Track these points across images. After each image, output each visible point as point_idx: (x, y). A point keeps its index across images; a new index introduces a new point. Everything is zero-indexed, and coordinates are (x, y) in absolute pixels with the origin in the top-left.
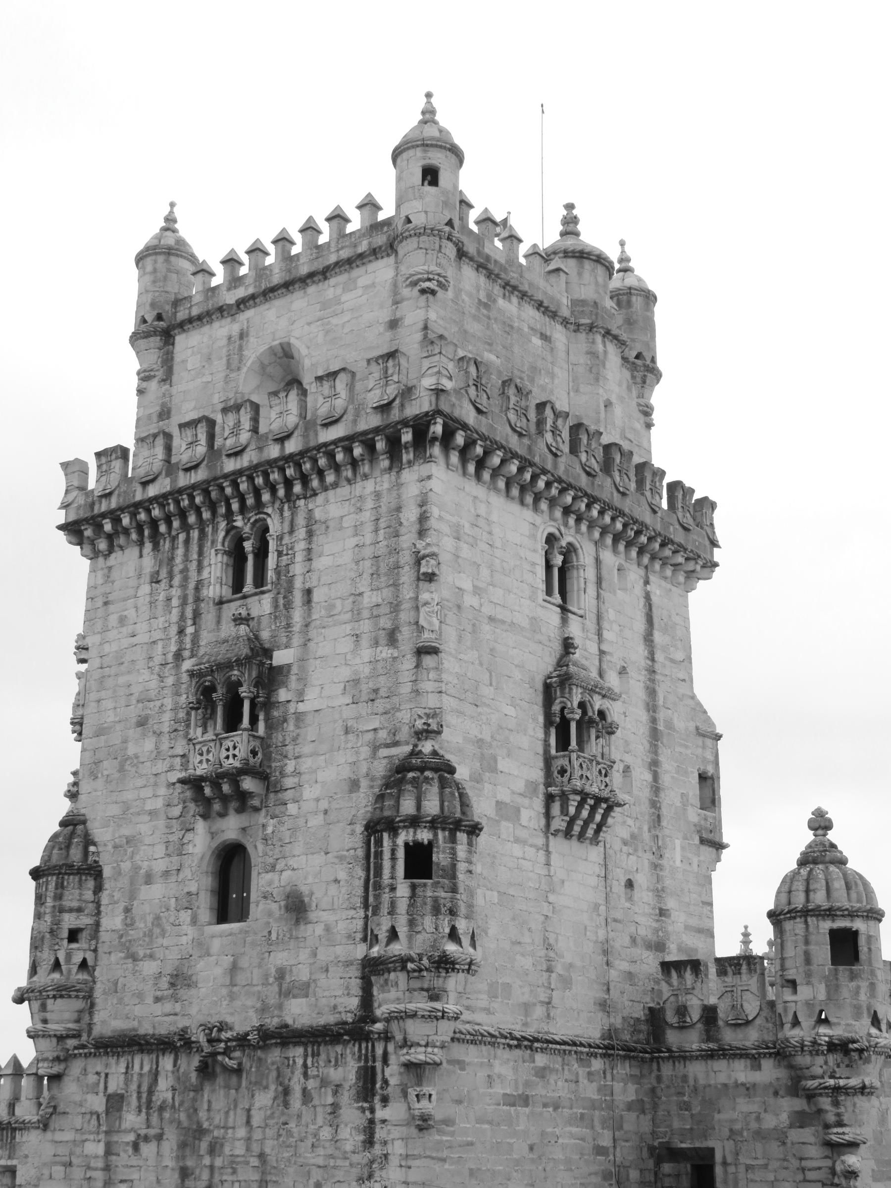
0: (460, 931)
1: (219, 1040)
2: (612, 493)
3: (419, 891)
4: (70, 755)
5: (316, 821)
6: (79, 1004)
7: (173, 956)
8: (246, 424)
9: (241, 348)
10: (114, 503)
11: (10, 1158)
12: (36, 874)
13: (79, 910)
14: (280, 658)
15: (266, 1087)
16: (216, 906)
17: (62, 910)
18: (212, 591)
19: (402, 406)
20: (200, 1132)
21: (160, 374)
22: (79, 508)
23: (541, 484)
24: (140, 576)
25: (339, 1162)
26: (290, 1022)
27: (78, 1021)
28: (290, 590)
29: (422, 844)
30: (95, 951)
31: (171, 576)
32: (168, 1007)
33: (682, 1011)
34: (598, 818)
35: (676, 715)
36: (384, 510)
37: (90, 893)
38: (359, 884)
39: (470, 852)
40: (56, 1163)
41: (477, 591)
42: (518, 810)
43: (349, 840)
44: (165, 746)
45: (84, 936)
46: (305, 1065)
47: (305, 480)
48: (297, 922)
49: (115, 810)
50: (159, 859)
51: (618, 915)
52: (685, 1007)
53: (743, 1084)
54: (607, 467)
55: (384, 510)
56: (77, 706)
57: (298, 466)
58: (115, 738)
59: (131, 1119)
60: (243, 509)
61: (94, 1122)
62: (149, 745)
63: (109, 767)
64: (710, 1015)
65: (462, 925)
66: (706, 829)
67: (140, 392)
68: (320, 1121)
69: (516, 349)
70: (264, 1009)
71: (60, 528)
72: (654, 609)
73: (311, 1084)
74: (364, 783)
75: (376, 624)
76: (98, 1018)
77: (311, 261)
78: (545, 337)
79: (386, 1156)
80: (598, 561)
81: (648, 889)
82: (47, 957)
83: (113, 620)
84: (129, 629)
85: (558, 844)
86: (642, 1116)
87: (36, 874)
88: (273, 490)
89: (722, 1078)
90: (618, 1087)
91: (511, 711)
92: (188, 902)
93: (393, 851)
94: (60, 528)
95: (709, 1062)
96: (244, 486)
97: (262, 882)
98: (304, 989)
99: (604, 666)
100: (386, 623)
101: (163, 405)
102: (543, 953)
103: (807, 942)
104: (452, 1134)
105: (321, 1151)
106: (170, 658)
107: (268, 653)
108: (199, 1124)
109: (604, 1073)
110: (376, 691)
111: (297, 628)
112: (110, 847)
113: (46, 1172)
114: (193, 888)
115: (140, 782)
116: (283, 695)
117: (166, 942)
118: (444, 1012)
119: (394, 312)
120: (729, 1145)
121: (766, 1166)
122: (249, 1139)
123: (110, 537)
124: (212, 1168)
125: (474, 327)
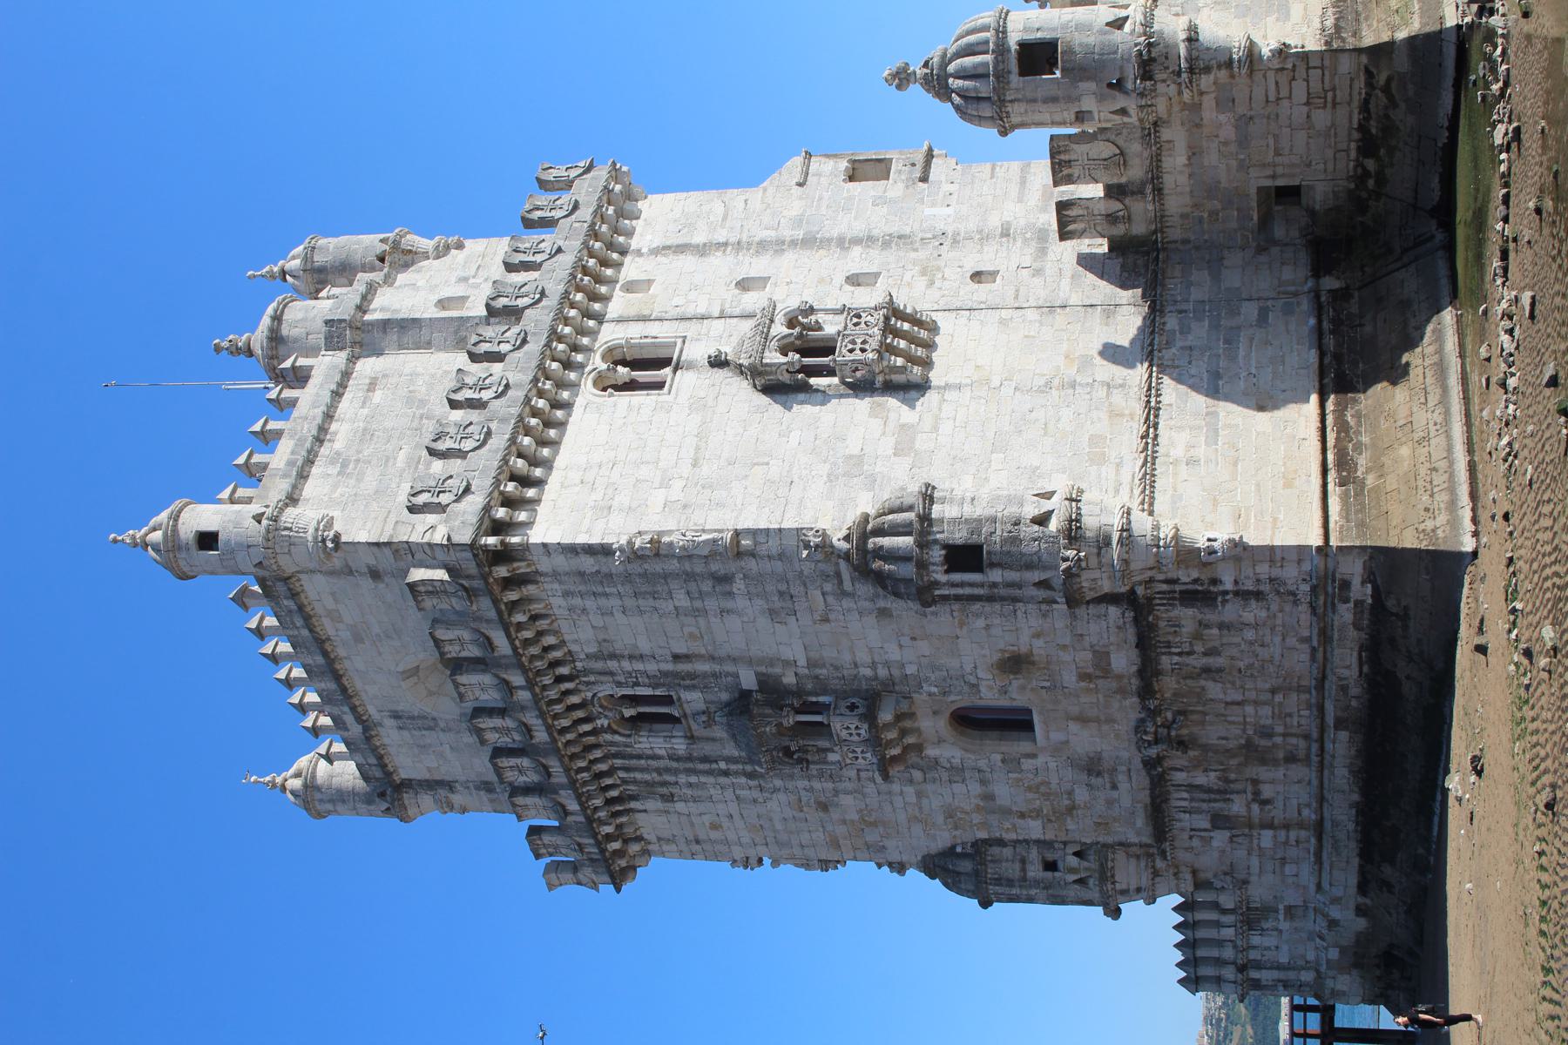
0: (1037, 512)
1: (1156, 733)
3: (995, 559)
4: (861, 874)
5: (924, 647)
6: (1120, 856)
7: (1069, 774)
8: (497, 722)
9: (413, 718)
11: (1277, 911)
12: (985, 904)
13: (1023, 861)
14: (748, 680)
15: (1203, 688)
16: (1015, 734)
17: (1024, 879)
18: (680, 746)
19: (468, 577)
20: (1249, 746)
21: (442, 792)
22: (596, 873)
23: (541, 403)
24: (667, 812)
25: (1279, 622)
26: (1135, 668)
27: (1138, 857)
28: (675, 675)
29: (947, 557)
30: (1065, 843)
31: (664, 784)
32: (1122, 778)
33: (1112, 218)
34: (906, 326)
35: (785, 213)
36: (582, 588)
37: (1005, 850)
38: (988, 608)
39: (952, 501)
40: (1282, 872)
41: (665, 484)
43: (942, 620)
44: (849, 786)
45: (1050, 856)
46: (1180, 654)
47: (555, 664)
48: (1033, 663)
49: (917, 829)
50: (970, 788)
51: (1011, 293)
53: (1189, 158)
55: (582, 588)
56: (807, 866)
57: (539, 673)
58: (841, 830)
59: (1237, 807)
61: (1240, 840)
62: (847, 800)
63: (872, 836)
64: (1113, 191)
65: (1031, 510)
67: (464, 810)
68: (1237, 640)
69: (388, 424)
70: (1122, 691)
71: (618, 890)
73: (1199, 648)
74: (881, 604)
75: (708, 594)
76: (1135, 840)
77: (310, 653)
78: (372, 386)
79: (1271, 580)
80: (619, 321)
81: (980, 252)
83: (714, 835)
84: (726, 823)
85: (935, 377)
86: (1226, 262)
87: (985, 904)
88: (567, 693)
89: (1183, 179)
90: (1196, 294)
91: (795, 437)
92: (1012, 763)
93: (954, 585)
94: (618, 890)
95: (1166, 191)
96: (565, 723)
97: (990, 695)
98: (1101, 658)
99: (737, 312)
100: (707, 586)
101: (478, 788)
103: (1034, 101)
105: (1267, 639)
106: (751, 783)
107: (745, 695)
108: (1241, 747)
109: (1180, 312)
110: (781, 594)
111: (717, 668)
112: (958, 833)
113: (1290, 880)
114: (999, 757)
115: (888, 808)
116: (789, 679)
117: (1054, 781)
118: (1122, 530)
119: (361, 574)
120: (1254, 173)
121: (1276, 137)
122: (1256, 703)
123: (626, 841)
124: (1284, 735)
125: (370, 481)
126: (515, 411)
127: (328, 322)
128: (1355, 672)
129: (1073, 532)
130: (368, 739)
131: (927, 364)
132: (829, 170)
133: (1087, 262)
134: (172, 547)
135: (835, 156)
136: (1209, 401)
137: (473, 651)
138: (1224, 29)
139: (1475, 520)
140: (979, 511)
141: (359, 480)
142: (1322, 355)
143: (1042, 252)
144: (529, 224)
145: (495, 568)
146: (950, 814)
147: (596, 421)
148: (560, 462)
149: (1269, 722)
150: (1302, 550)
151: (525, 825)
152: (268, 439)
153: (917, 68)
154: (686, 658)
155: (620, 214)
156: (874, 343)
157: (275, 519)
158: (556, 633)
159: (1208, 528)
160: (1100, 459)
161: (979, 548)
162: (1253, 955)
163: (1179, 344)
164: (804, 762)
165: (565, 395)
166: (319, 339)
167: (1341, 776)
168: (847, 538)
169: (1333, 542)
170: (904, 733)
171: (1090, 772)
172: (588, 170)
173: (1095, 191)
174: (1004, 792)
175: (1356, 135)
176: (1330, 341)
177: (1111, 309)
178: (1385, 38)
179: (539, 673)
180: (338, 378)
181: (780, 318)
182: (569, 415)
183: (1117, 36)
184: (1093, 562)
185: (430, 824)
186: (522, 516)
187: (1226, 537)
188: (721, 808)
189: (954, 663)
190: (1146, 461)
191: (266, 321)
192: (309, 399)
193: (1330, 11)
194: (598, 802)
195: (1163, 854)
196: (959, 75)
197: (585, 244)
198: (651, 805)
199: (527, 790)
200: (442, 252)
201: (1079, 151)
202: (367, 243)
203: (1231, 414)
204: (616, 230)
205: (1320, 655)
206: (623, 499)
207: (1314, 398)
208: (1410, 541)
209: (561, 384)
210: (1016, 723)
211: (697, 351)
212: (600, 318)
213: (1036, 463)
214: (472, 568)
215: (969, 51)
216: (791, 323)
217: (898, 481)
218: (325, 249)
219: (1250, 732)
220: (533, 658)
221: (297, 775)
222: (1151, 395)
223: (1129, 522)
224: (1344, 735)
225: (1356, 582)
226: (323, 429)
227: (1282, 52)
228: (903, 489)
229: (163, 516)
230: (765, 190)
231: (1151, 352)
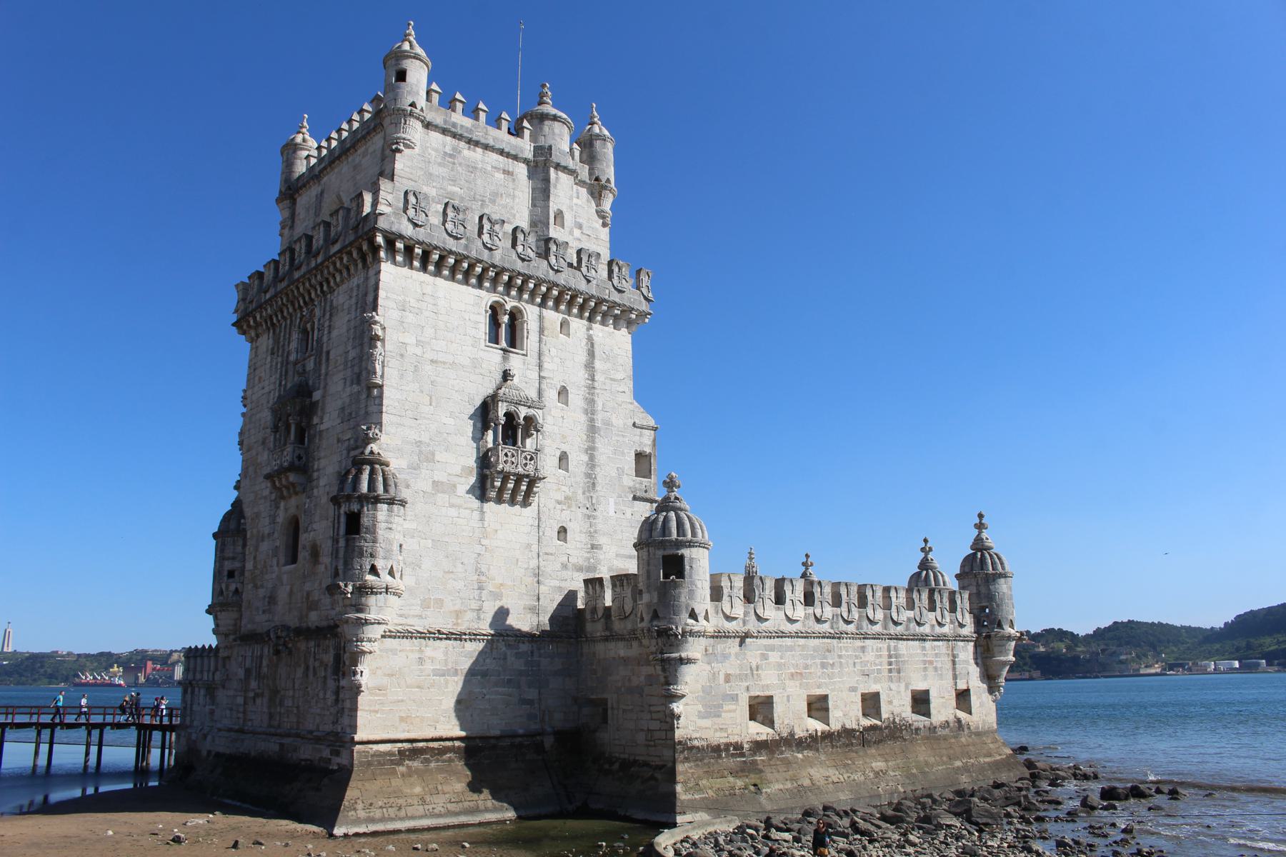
4: (232, 465)
6: (235, 615)
7: (270, 586)
12: (215, 536)
14: (317, 396)
18: (292, 358)
23: (478, 270)
33: (594, 610)
34: (524, 488)
41: (419, 343)
42: (455, 486)
47: (328, 283)
50: (266, 524)
51: (550, 551)
54: (545, 254)
56: (241, 434)
59: (253, 684)
62: (266, 457)
63: (251, 469)
65: (380, 564)
67: (281, 235)
69: (479, 182)
78: (507, 172)
80: (541, 317)
87: (215, 536)
91: (451, 421)
97: (304, 538)
98: (313, 606)
99: (544, 386)
100: (356, 369)
104: (385, 695)
107: (310, 395)
116: (316, 420)
117: (267, 577)
122: (293, 697)
123: (256, 329)
126: (474, 254)
127: (550, 147)
128: (303, 757)
129: (364, 590)
130: (312, 178)
131: (499, 500)
132: (645, 442)
133: (572, 595)
134: (401, 55)
135: (654, 445)
136: (465, 672)
137: (333, 234)
138: (691, 681)
139: (357, 835)
140: (381, 532)
141: (440, 164)
142: (497, 738)
143: (579, 569)
144: (610, 264)
146: (258, 515)
147: (468, 304)
148: (439, 281)
150: (354, 728)
151: (262, 270)
152: (473, 113)
153: (676, 493)
154: (328, 359)
155: (616, 318)
156: (508, 468)
157: (411, 114)
158: (342, 281)
159: (367, 673)
160: (425, 605)
161: (357, 531)
163: (509, 653)
164: (276, 429)
165: (487, 284)
166: (542, 141)
168: (372, 452)
169: (358, 747)
172: (646, 299)
173: (608, 602)
174: (265, 547)
175: (632, 758)
176: (507, 742)
177: (535, 610)
178: (679, 778)
180: (513, 152)
181: (531, 412)
182: (473, 287)
183: (684, 615)
184: (347, 602)
186: (399, 258)
187: (363, 683)
189: (317, 518)
191: (554, 111)
192: (501, 137)
193: (705, 743)
195: (235, 640)
196: (666, 520)
197: (593, 297)
198: (271, 341)
199: (277, 269)
200: (601, 214)
201: (628, 592)
202: (608, 171)
203: (455, 686)
204: (605, 315)
206: (410, 318)
207: (463, 734)
208: (351, 794)
209: (495, 281)
212: (543, 305)
215: (680, 525)
216: (528, 419)
218: (604, 146)
220: (328, 267)
221: (304, 140)
222: (474, 636)
224: (277, 748)
225: (338, 760)
226: (477, 144)
227: (674, 717)
228: (408, 486)
229: (419, 50)
231: (501, 635)
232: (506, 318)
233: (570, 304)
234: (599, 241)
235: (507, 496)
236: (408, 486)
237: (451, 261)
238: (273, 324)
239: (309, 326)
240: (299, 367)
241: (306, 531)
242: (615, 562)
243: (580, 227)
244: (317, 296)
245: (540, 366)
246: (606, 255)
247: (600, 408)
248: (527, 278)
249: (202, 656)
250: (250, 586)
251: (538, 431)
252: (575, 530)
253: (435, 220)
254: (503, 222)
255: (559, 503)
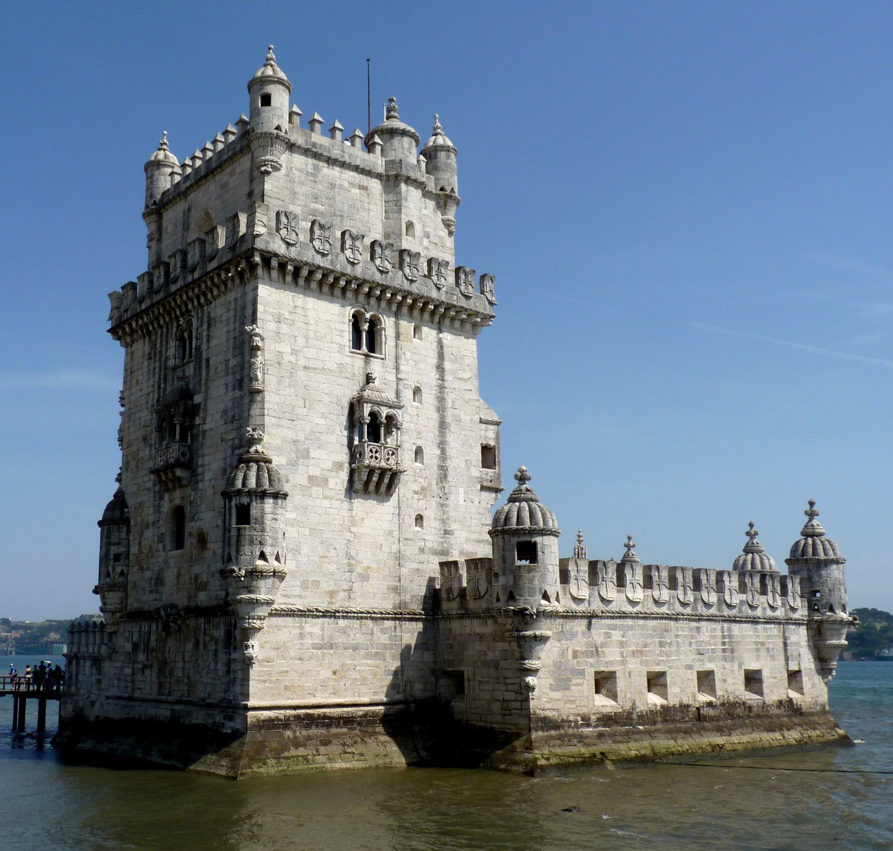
2: (403, 282)
4: (115, 459)
5: (210, 492)
7: (156, 568)
8: (179, 265)
10: (129, 314)
11: (99, 675)
12: (100, 524)
13: (119, 544)
14: (198, 399)
23: (342, 283)
26: (199, 604)
27: (121, 603)
30: (128, 565)
33: (450, 590)
35: (462, 412)
39: (275, 508)
41: (294, 352)
43: (219, 502)
45: (122, 557)
49: (135, 488)
52: (451, 589)
56: (120, 431)
58: (135, 448)
59: (142, 656)
60: (182, 314)
62: (147, 452)
63: (132, 464)
64: (463, 593)
65: (268, 550)
66: (486, 480)
67: (149, 247)
70: (190, 597)
71: (109, 331)
72: (445, 349)
81: (435, 519)
82: (104, 570)
83: (134, 381)
84: (139, 387)
87: (100, 524)
91: (323, 421)
92: (161, 538)
94: (109, 331)
97: (190, 527)
98: (202, 587)
99: (401, 387)
100: (238, 376)
102: (346, 561)
104: (272, 666)
105: (211, 676)
107: (191, 397)
108: (166, 659)
109: (395, 628)
110: (234, 416)
111: (203, 382)
114: (164, 532)
116: (198, 421)
117: (154, 561)
122: (184, 668)
123: (131, 335)
124: (170, 682)
126: (338, 268)
128: (195, 721)
129: (255, 574)
132: (489, 435)
140: (268, 522)
143: (436, 553)
144: (457, 271)
145: (246, 263)
146: (141, 505)
149: (176, 674)
150: (246, 696)
151: (136, 281)
154: (208, 366)
155: (463, 321)
156: (374, 463)
158: (219, 296)
159: (256, 647)
160: (305, 585)
162: (82, 662)
164: (160, 429)
167: (151, 711)
168: (257, 451)
170: (173, 481)
171: (157, 579)
174: (149, 533)
179: (199, 286)
184: (241, 585)
185: (142, 230)
188: (145, 385)
189: (203, 508)
190: (302, 611)
194: (145, 319)
195: (121, 617)
199: (151, 282)
200: (447, 224)
205: (202, 703)
206: (285, 329)
210: (179, 544)
211: (376, 367)
213: (302, 552)
214: (244, 248)
216: (390, 418)
217: (293, 480)
219: (172, 664)
220: (206, 282)
223: (263, 604)
224: (168, 713)
225: (231, 724)
228: (288, 481)
230: (478, 400)
232: (366, 327)
233: (423, 310)
234: (445, 249)
235: (372, 487)
236: (288, 481)
237: (319, 276)
238: (149, 333)
239: (186, 334)
240: (179, 373)
241: (192, 519)
242: (465, 546)
243: (428, 237)
244: (194, 307)
245: (397, 369)
246: (452, 266)
247: (450, 405)
248: (384, 289)
249: (86, 631)
250: (136, 569)
251: (398, 429)
252: (430, 515)
253: (303, 237)
254: (363, 237)
255: (416, 493)
